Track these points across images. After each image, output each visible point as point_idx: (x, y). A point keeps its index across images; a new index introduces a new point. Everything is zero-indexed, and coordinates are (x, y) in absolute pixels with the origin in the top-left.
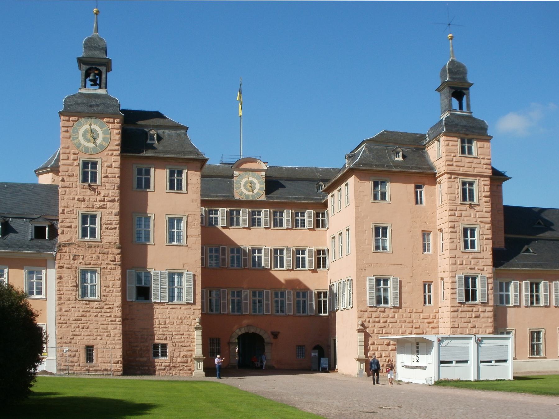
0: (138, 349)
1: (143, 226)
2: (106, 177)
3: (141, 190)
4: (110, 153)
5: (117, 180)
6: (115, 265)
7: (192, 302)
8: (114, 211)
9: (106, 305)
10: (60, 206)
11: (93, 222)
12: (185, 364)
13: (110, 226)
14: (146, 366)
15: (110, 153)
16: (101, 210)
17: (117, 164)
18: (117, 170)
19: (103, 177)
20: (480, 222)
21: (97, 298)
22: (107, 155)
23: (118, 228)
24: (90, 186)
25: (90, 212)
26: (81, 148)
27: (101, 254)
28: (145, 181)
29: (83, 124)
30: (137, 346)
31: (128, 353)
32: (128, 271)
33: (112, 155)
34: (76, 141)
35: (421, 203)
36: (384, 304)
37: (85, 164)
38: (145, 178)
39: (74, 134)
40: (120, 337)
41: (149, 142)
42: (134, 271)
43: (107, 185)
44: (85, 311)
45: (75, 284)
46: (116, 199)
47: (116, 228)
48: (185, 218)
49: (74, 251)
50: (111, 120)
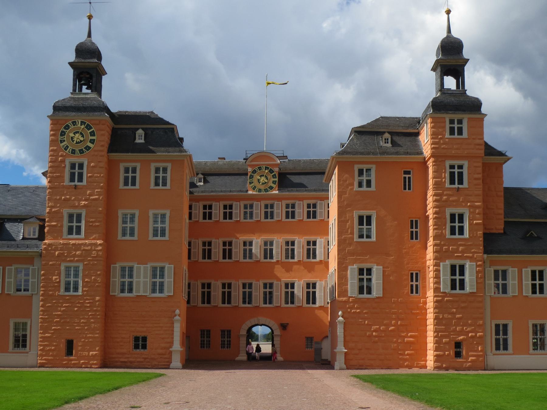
29: (71, 127)
35: (409, 189)
37: (73, 166)
39: (62, 137)
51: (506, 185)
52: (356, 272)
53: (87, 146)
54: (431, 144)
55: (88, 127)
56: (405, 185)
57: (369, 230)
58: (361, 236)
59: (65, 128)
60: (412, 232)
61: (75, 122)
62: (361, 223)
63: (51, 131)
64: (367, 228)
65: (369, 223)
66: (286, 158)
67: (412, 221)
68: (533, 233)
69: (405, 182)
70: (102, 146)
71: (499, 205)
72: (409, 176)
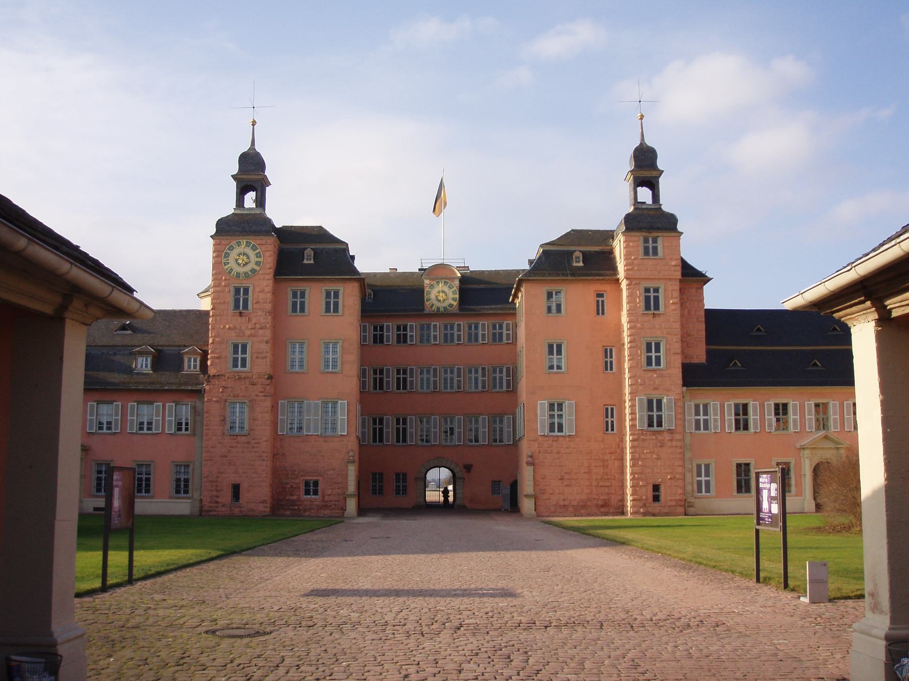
0: (288, 486)
1: (297, 353)
2: (256, 303)
3: (296, 314)
4: (262, 277)
5: (269, 307)
6: (264, 396)
7: (346, 434)
8: (265, 339)
9: (253, 439)
10: (210, 335)
11: (244, 351)
12: (337, 503)
13: (260, 355)
14: (296, 505)
15: (262, 277)
16: (252, 338)
17: (269, 289)
18: (269, 296)
19: (254, 302)
20: (667, 334)
21: (245, 432)
22: (259, 279)
23: (269, 357)
24: (240, 313)
25: (240, 341)
26: (232, 273)
27: (250, 385)
28: (300, 304)
30: (287, 483)
31: (278, 490)
32: (280, 402)
33: (264, 279)
34: (226, 267)
35: (603, 313)
36: (558, 432)
37: (237, 290)
38: (300, 301)
40: (267, 474)
41: (305, 262)
42: (286, 401)
43: (259, 311)
44: (232, 447)
45: (222, 418)
46: (268, 325)
47: (266, 357)
48: (340, 342)
49: (224, 383)
50: (263, 242)
51: (706, 308)
52: (547, 406)
53: (253, 269)
54: (625, 266)
55: (254, 248)
56: (598, 310)
57: (560, 360)
58: (551, 367)
59: (229, 249)
60: (606, 362)
61: (240, 242)
62: (551, 352)
63: (214, 252)
64: (557, 358)
65: (559, 352)
66: (467, 268)
67: (606, 350)
68: (737, 362)
69: (598, 306)
70: (269, 268)
71: (699, 329)
72: (602, 299)
